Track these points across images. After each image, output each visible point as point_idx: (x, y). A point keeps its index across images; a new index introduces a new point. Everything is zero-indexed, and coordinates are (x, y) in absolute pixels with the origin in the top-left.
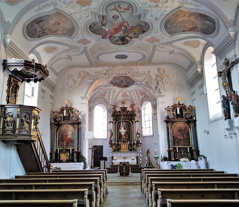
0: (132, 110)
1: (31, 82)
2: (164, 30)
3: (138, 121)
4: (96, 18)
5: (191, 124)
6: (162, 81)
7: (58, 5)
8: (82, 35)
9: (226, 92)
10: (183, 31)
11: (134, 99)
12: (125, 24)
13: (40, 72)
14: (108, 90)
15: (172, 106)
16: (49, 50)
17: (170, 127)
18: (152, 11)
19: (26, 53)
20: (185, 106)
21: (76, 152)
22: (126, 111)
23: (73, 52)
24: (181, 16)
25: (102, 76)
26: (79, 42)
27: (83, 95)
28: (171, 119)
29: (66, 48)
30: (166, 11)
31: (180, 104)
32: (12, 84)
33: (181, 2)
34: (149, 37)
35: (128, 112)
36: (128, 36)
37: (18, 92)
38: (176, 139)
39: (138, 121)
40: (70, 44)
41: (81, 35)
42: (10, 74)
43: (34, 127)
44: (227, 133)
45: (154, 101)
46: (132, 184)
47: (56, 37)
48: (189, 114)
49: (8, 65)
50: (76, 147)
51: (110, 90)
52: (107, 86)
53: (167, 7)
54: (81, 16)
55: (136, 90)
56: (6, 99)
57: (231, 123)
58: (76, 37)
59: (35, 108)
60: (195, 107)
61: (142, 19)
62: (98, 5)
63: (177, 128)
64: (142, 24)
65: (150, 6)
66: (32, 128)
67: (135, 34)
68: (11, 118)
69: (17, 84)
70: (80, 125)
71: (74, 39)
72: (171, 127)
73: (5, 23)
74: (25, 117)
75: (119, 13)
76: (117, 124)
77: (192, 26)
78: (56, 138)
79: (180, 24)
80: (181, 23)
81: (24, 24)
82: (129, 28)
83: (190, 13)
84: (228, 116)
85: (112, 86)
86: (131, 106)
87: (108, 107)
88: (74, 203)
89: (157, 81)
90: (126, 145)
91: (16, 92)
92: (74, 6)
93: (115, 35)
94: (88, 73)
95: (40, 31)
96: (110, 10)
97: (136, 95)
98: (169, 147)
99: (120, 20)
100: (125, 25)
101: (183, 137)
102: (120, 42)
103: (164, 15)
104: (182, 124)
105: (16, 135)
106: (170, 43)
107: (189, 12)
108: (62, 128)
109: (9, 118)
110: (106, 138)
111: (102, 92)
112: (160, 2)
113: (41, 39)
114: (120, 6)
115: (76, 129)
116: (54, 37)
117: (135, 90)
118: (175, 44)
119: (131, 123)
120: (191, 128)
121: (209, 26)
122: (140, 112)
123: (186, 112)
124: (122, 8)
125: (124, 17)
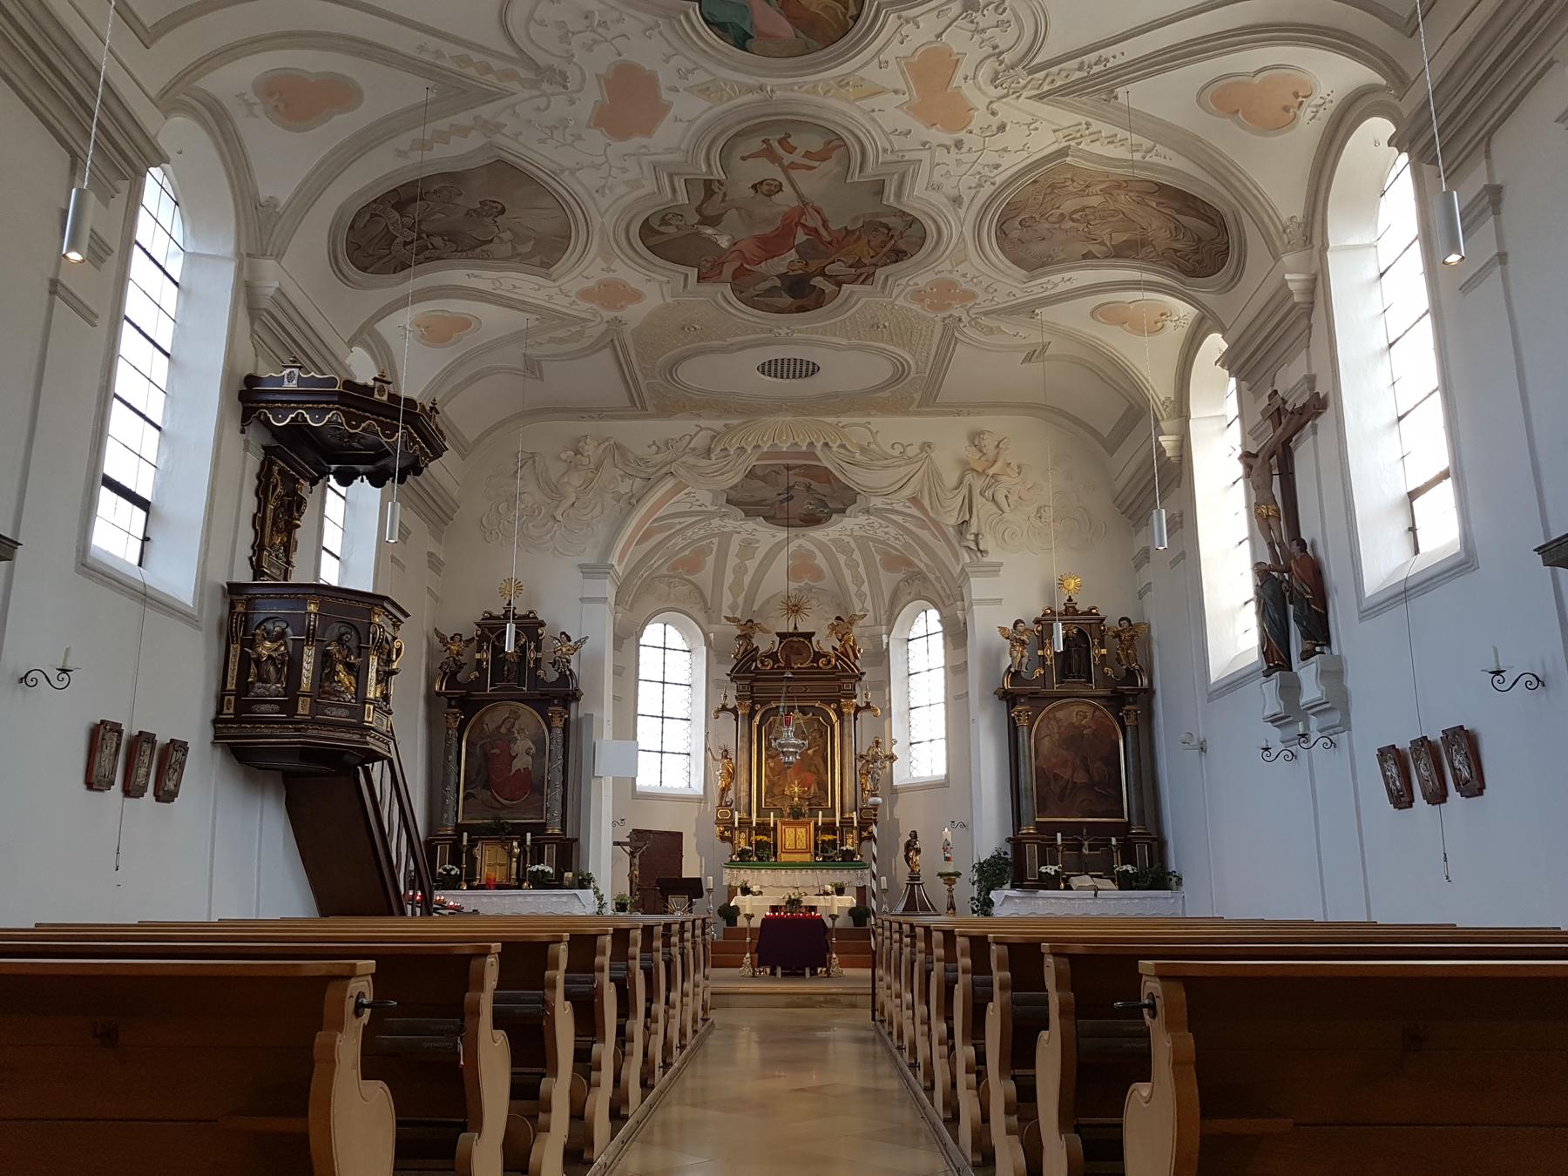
0: (838, 644)
1: (357, 482)
2: (992, 250)
3: (868, 706)
4: (674, 191)
5: (1127, 707)
6: (988, 493)
7: (504, 131)
8: (604, 265)
9: (1271, 545)
10: (1085, 257)
11: (853, 589)
12: (812, 221)
13: (410, 433)
14: (715, 540)
15: (1037, 621)
16: (436, 333)
17: (1023, 723)
18: (934, 166)
19: (337, 345)
20: (1102, 620)
21: (553, 839)
23: (551, 340)
24: (1070, 188)
25: (691, 460)
26: (586, 295)
27: (589, 558)
28: (1029, 682)
29: (519, 320)
30: (1000, 169)
31: (1075, 612)
32: (275, 488)
33: (1066, 132)
34: (923, 279)
35: (818, 655)
36: (823, 274)
37: (299, 526)
39: (868, 706)
40: (547, 305)
41: (600, 263)
42: (268, 440)
43: (379, 690)
44: (1274, 735)
45: (956, 601)
46: (831, 1000)
47: (476, 272)
48: (1119, 660)
49: (267, 402)
50: (557, 813)
51: (725, 538)
52: (712, 515)
53: (1005, 150)
54: (604, 181)
55: (862, 542)
56: (250, 559)
57: (1290, 690)
58: (577, 272)
59: (386, 605)
60: (1149, 626)
61: (890, 198)
62: (690, 133)
63: (1059, 727)
64: (892, 221)
65: (924, 144)
66: (371, 695)
67: (858, 264)
68: (275, 646)
69: (295, 493)
70: (573, 705)
71: (562, 281)
73: (258, 206)
74: (340, 641)
75: (785, 170)
76: (757, 718)
77: (1125, 237)
78: (453, 767)
79: (1068, 225)
80: (1073, 220)
81: (342, 210)
82: (829, 239)
83: (1114, 178)
84: (1280, 658)
85: (736, 520)
86: (833, 627)
87: (715, 627)
88: (603, 937)
89: (964, 491)
91: (291, 527)
92: (578, 137)
93: (763, 267)
94: (618, 446)
95: (406, 244)
96: (744, 159)
97: (861, 569)
98: (1017, 822)
99: (786, 200)
100: (810, 223)
101: (1088, 771)
102: (787, 300)
103: (993, 184)
104: (1084, 708)
105: (300, 723)
106: (1028, 309)
107: (1108, 174)
108: (487, 719)
109: (268, 644)
110: (702, 793)
111: (683, 548)
112: (969, 128)
113: (407, 279)
114: (789, 140)
115: (558, 723)
116: (469, 272)
117: (856, 539)
118: (1046, 314)
119: (834, 718)
120: (1129, 729)
121: (1200, 239)
122: (881, 657)
123: (1104, 651)
124: (800, 151)
125: (804, 189)
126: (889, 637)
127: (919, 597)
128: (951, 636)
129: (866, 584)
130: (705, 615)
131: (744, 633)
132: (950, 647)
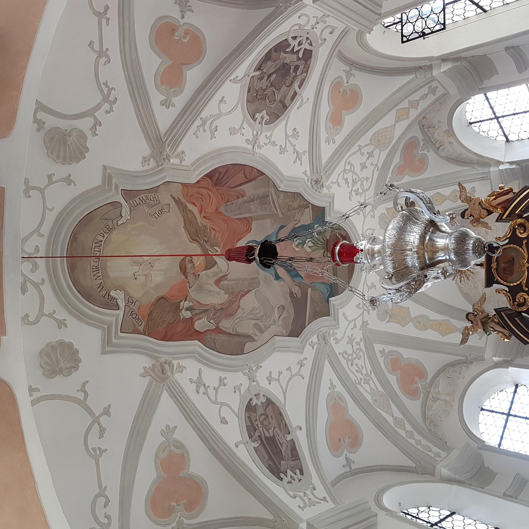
0: (495, 215)
14: (378, 347)
22: (514, 254)
35: (514, 239)
45: (433, 79)
111: (385, 383)
126: (503, 163)
127: (450, 132)
128: (482, 82)
129: (440, 191)
130: (474, 363)
131: (480, 323)
132: (494, 80)
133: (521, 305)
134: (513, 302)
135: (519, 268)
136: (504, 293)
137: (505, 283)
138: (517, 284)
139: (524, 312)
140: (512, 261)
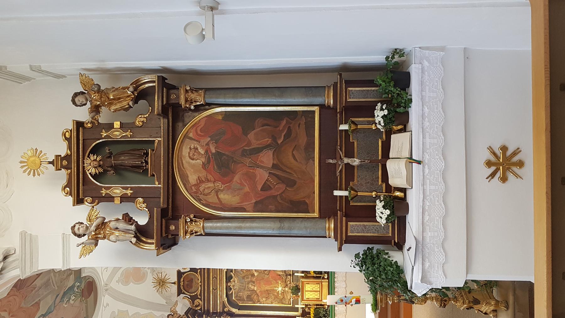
22: (193, 277)
31: (67, 157)
38: (273, 192)
72: (201, 223)
90: (308, 287)
133: (197, 306)
134: (193, 305)
135: (195, 284)
136: (188, 300)
137: (188, 294)
138: (195, 295)
139: (198, 310)
140: (191, 281)
